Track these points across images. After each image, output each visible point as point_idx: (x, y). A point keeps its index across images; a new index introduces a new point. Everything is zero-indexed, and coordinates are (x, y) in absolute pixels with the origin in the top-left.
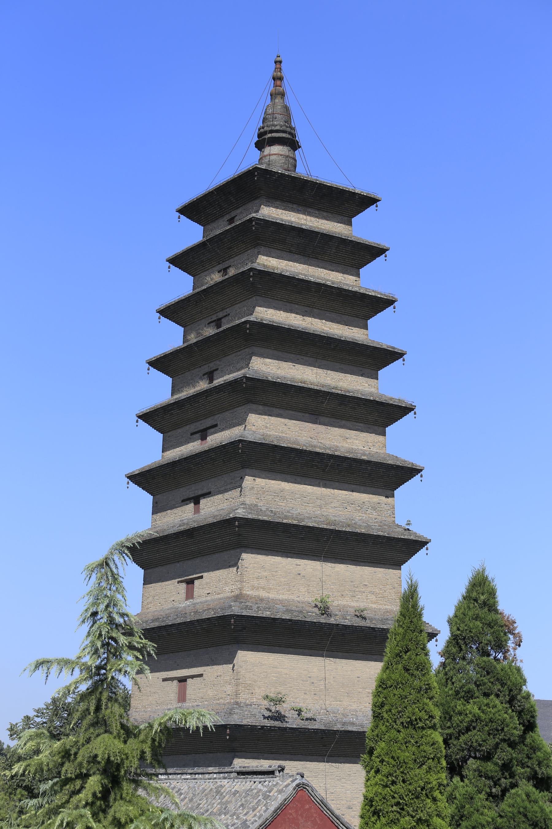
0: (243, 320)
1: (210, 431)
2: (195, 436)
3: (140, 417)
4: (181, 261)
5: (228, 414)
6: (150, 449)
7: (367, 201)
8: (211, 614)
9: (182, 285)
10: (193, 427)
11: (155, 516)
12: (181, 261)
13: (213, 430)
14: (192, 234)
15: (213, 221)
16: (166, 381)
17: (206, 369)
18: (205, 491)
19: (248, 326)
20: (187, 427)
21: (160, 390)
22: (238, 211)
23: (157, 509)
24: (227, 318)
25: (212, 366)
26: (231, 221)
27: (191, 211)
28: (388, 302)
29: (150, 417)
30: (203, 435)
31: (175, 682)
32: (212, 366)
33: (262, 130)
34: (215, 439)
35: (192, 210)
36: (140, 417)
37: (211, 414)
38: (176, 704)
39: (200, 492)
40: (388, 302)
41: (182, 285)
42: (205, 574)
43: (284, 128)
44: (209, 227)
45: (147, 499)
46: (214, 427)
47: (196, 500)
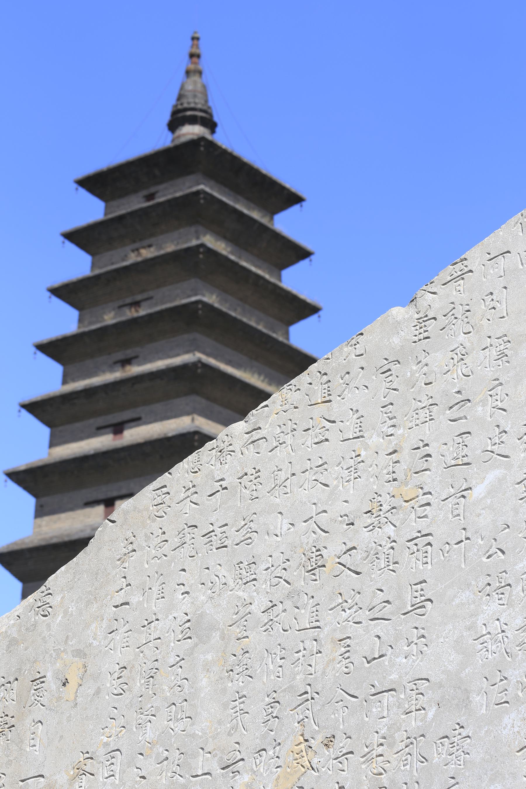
0: (193, 299)
1: (126, 425)
2: (103, 431)
4: (79, 237)
5: (158, 407)
6: (35, 445)
7: (293, 199)
10: (101, 421)
11: (39, 520)
12: (79, 237)
13: (132, 424)
15: (121, 196)
16: (55, 369)
17: (120, 355)
18: (124, 492)
19: (200, 306)
20: (91, 421)
21: (49, 379)
22: (161, 187)
23: (40, 512)
24: (149, 302)
25: (130, 353)
26: (150, 197)
27: (95, 184)
28: (314, 310)
29: (36, 408)
30: (118, 429)
32: (130, 353)
33: (180, 107)
34: (134, 435)
35: (95, 184)
37: (134, 405)
39: (115, 494)
40: (314, 310)
43: (205, 108)
44: (114, 203)
45: (28, 501)
46: (136, 421)
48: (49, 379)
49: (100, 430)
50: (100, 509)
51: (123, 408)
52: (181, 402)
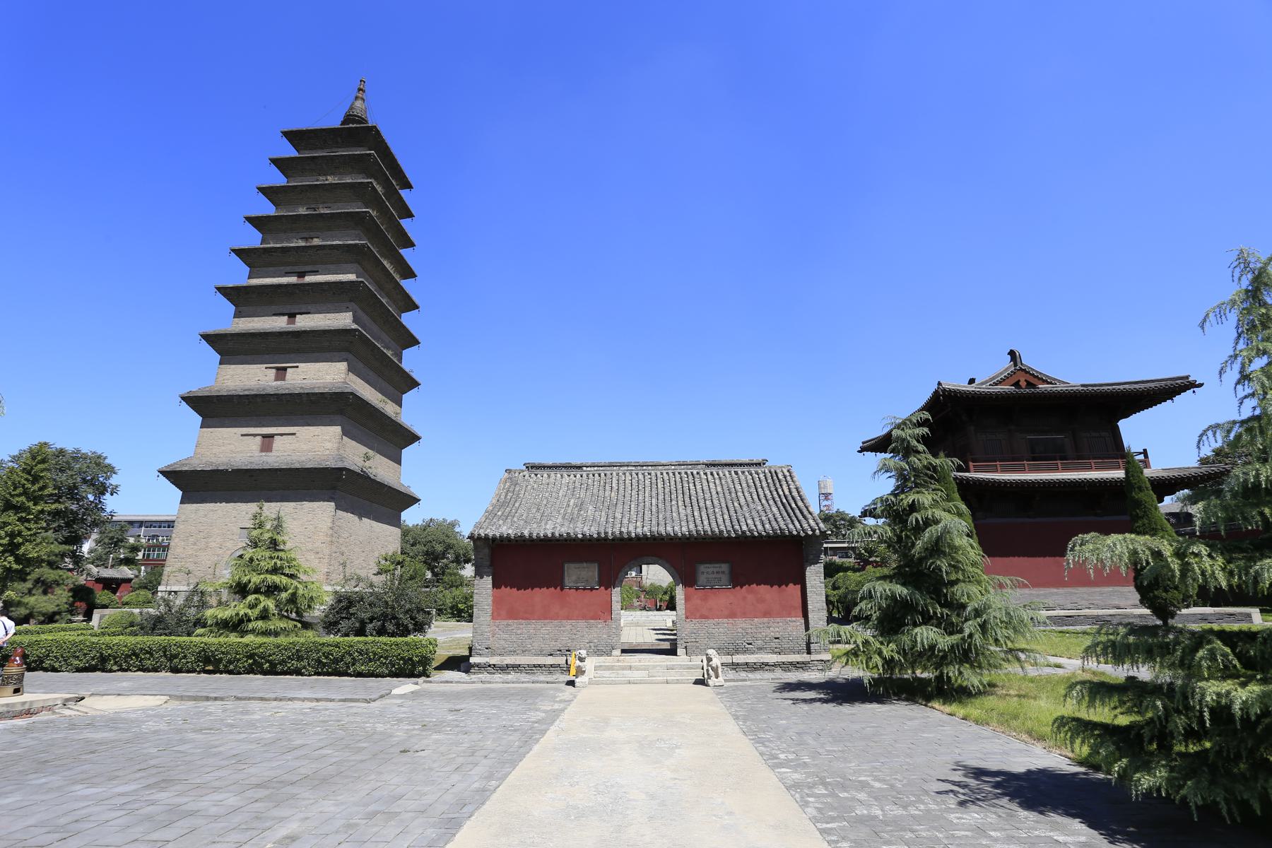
3: (234, 251)
4: (278, 163)
5: (332, 267)
8: (327, 390)
9: (277, 179)
10: (288, 269)
14: (289, 151)
17: (305, 235)
27: (294, 137)
30: (301, 275)
31: (259, 438)
34: (309, 279)
35: (294, 137)
36: (234, 251)
38: (257, 453)
41: (277, 179)
42: (300, 365)
46: (315, 272)
47: (292, 316)
48: (253, 239)
49: (287, 274)
50: (286, 318)
51: (306, 264)
52: (349, 265)
